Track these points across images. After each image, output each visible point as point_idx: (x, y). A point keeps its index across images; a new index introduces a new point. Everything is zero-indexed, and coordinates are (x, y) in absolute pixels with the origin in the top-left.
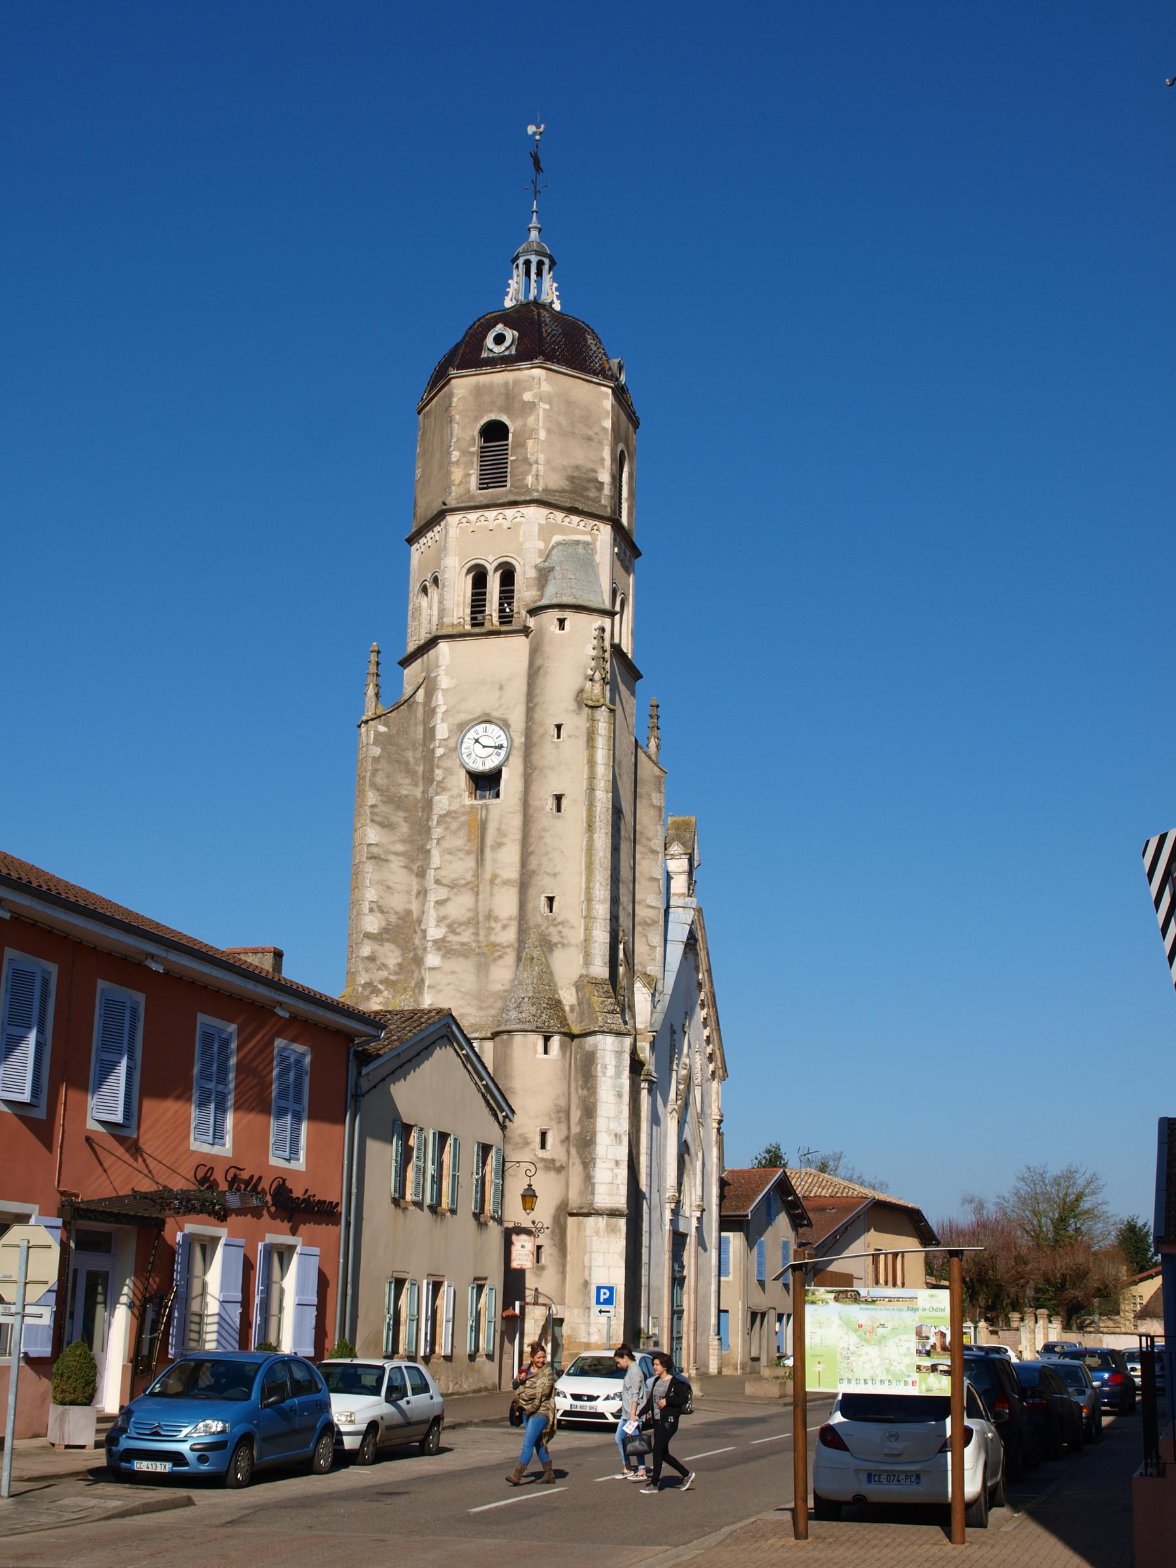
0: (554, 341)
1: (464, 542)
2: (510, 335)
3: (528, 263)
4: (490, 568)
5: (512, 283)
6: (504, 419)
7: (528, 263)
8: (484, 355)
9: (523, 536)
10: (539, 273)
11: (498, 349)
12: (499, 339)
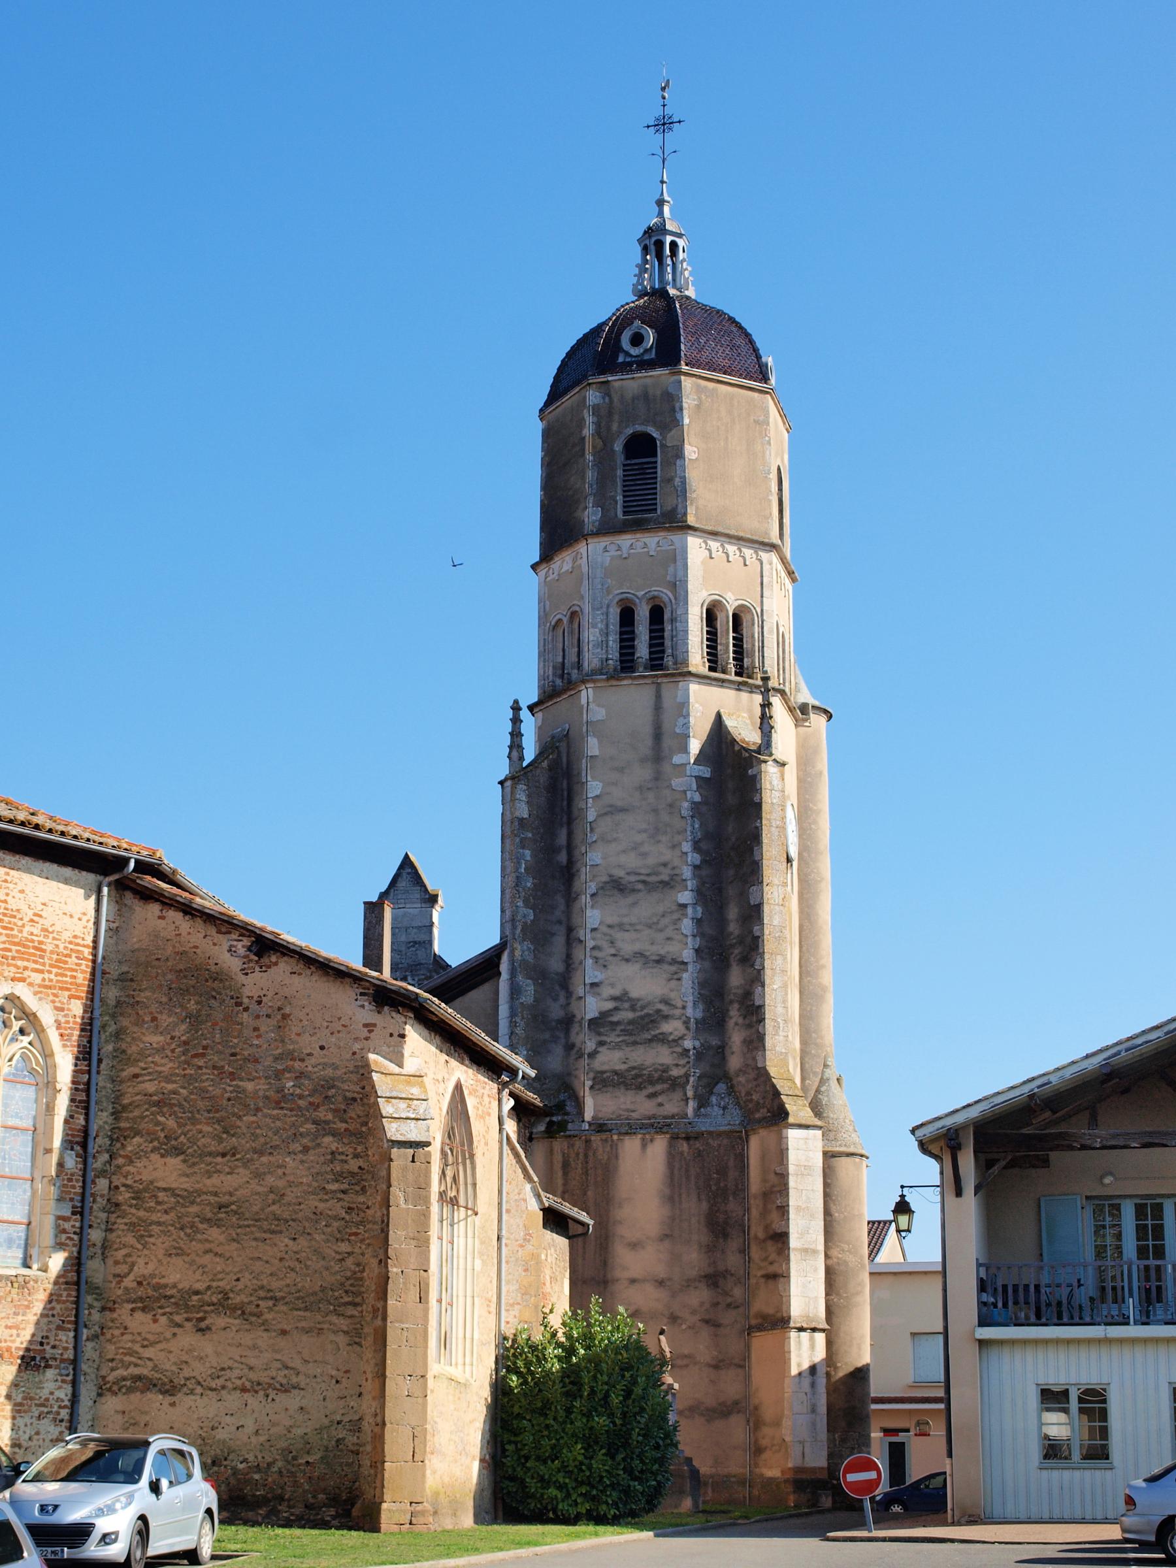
8: (621, 359)
11: (635, 351)
12: (637, 339)
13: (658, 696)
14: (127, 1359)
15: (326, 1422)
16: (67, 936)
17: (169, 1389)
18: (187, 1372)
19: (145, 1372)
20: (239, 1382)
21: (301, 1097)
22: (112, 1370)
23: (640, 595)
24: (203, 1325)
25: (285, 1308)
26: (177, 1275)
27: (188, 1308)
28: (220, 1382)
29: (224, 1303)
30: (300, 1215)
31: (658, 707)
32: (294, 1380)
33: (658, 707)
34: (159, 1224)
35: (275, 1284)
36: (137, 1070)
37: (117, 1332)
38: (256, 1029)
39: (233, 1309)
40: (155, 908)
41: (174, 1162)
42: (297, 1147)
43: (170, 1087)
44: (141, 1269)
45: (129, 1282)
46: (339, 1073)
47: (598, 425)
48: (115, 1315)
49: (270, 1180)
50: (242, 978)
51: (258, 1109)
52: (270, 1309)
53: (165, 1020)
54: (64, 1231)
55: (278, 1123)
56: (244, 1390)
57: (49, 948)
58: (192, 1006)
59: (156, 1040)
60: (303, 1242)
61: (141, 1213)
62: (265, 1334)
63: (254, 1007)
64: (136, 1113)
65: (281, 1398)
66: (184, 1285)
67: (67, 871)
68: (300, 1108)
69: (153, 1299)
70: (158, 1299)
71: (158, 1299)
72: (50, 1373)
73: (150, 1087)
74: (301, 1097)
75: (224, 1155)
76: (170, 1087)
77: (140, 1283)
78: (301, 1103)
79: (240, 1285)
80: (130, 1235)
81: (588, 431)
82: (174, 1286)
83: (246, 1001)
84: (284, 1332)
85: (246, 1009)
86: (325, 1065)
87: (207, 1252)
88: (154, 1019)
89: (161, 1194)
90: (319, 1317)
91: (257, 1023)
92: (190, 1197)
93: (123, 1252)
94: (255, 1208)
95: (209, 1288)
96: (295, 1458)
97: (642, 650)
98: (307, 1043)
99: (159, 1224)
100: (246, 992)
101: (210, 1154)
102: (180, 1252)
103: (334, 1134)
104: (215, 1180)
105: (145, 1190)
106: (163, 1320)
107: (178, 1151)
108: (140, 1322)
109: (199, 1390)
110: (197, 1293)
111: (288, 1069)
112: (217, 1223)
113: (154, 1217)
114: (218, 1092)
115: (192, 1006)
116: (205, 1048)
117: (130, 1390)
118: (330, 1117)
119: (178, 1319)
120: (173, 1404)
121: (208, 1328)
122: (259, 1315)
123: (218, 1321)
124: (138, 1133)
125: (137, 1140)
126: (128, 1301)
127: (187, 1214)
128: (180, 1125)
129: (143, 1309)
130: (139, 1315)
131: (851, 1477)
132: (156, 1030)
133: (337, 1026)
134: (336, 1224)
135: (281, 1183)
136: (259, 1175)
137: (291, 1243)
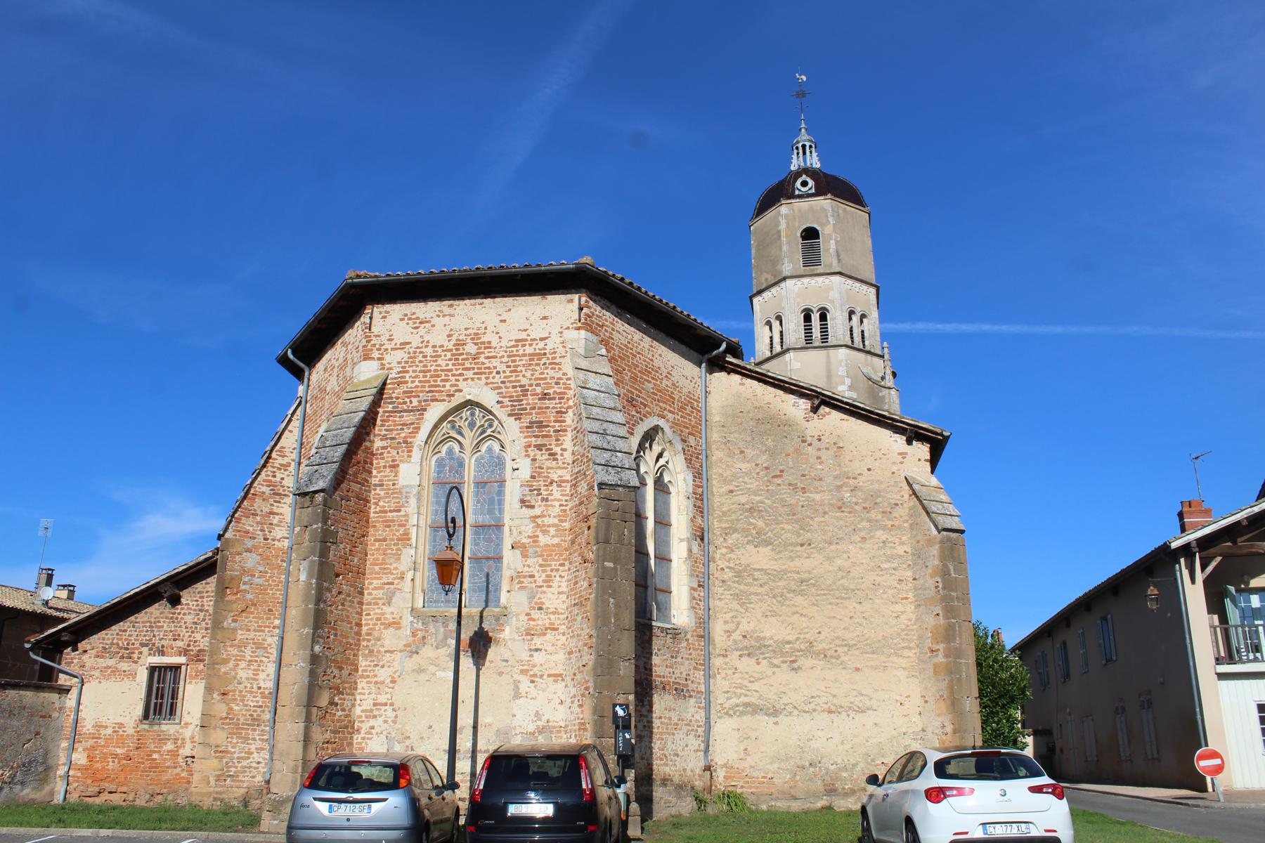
0: (828, 185)
1: (792, 296)
2: (811, 183)
3: (804, 146)
4: (815, 310)
5: (795, 156)
6: (815, 226)
7: (804, 146)
9: (832, 292)
10: (804, 153)
11: (804, 189)
12: (804, 184)
13: (828, 356)
14: (739, 691)
15: (895, 733)
16: (685, 390)
17: (775, 712)
18: (785, 700)
19: (753, 700)
20: (826, 707)
21: (856, 504)
22: (728, 699)
23: (815, 306)
24: (795, 665)
25: (857, 652)
26: (773, 630)
27: (783, 654)
28: (811, 706)
29: (810, 649)
30: (863, 587)
31: (828, 363)
32: (868, 703)
33: (828, 363)
34: (756, 594)
35: (848, 635)
36: (731, 488)
37: (730, 672)
38: (819, 458)
39: (818, 654)
40: (736, 378)
41: (765, 551)
42: (856, 538)
43: (758, 498)
44: (745, 627)
45: (737, 636)
46: (883, 486)
47: (787, 223)
48: (727, 660)
49: (838, 562)
50: (805, 424)
51: (825, 513)
52: (846, 653)
53: (750, 452)
54: (694, 598)
55: (841, 523)
56: (830, 712)
57: (676, 397)
58: (770, 443)
59: (745, 466)
60: (867, 605)
61: (742, 587)
62: (844, 672)
63: (815, 442)
64: (734, 517)
65: (859, 716)
66: (779, 637)
67: (683, 348)
68: (856, 511)
69: (754, 648)
70: (760, 648)
71: (760, 648)
72: (692, 701)
73: (743, 499)
74: (856, 504)
75: (802, 545)
76: (758, 498)
77: (744, 637)
78: (857, 507)
79: (822, 637)
80: (735, 603)
81: (783, 226)
82: (771, 638)
83: (809, 439)
84: (857, 669)
85: (810, 445)
86: (872, 482)
87: (794, 613)
88: (742, 452)
89: (757, 574)
90: (883, 658)
91: (819, 454)
92: (778, 575)
93: (731, 614)
94: (829, 582)
95: (798, 639)
96: (873, 760)
97: (816, 333)
98: (858, 467)
99: (756, 594)
100: (809, 433)
101: (791, 544)
102: (774, 614)
103: (884, 528)
104: (797, 563)
105: (744, 571)
106: (764, 662)
107: (767, 543)
108: (746, 664)
109: (796, 712)
110: (789, 643)
111: (845, 484)
112: (802, 593)
113: (752, 590)
114: (793, 502)
115: (770, 443)
116: (782, 471)
117: (742, 714)
118: (879, 517)
119: (776, 661)
120: (776, 723)
121: (800, 668)
122: (838, 658)
123: (806, 662)
124: (735, 531)
125: (735, 536)
126: (737, 650)
127: (778, 587)
128: (767, 525)
129: (749, 655)
130: (745, 659)
131: (1203, 763)
132: (745, 459)
133: (879, 454)
134: (891, 592)
135: (847, 564)
136: (830, 559)
137: (858, 606)
